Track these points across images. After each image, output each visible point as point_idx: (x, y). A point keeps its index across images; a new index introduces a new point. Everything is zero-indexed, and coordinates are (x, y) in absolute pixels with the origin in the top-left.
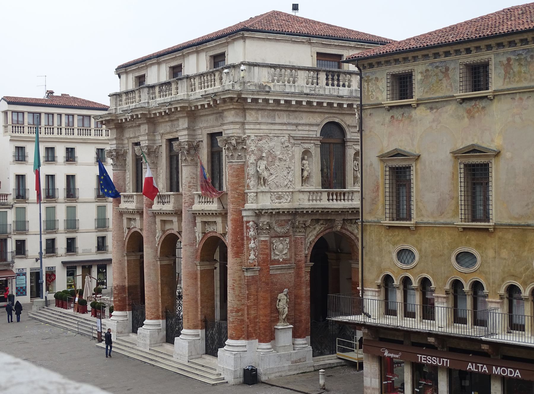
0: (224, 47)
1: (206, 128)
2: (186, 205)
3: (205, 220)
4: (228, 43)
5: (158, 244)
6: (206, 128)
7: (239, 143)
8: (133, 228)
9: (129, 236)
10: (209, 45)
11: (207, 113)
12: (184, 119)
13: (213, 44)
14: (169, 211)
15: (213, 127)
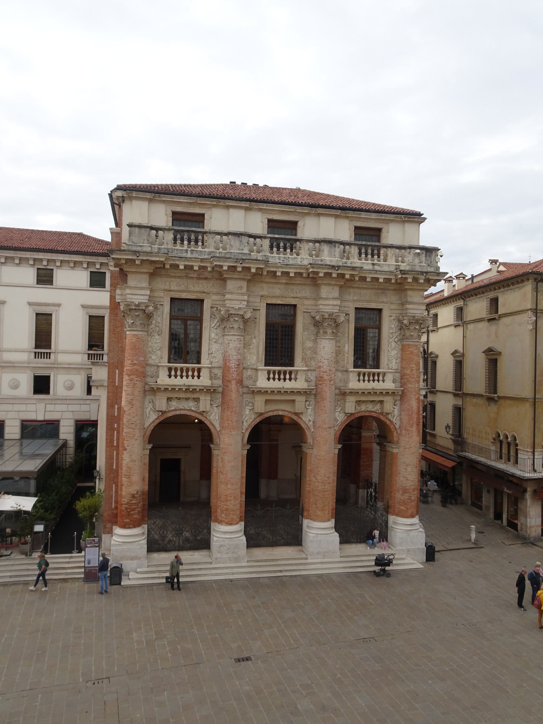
0: (383, 223)
1: (354, 301)
2: (332, 382)
3: (363, 398)
4: (392, 221)
5: (247, 430)
6: (354, 301)
7: (412, 323)
8: (173, 410)
9: (158, 421)
10: (363, 215)
11: (365, 286)
12: (332, 287)
13: (374, 216)
14: (303, 389)
15: (370, 301)
